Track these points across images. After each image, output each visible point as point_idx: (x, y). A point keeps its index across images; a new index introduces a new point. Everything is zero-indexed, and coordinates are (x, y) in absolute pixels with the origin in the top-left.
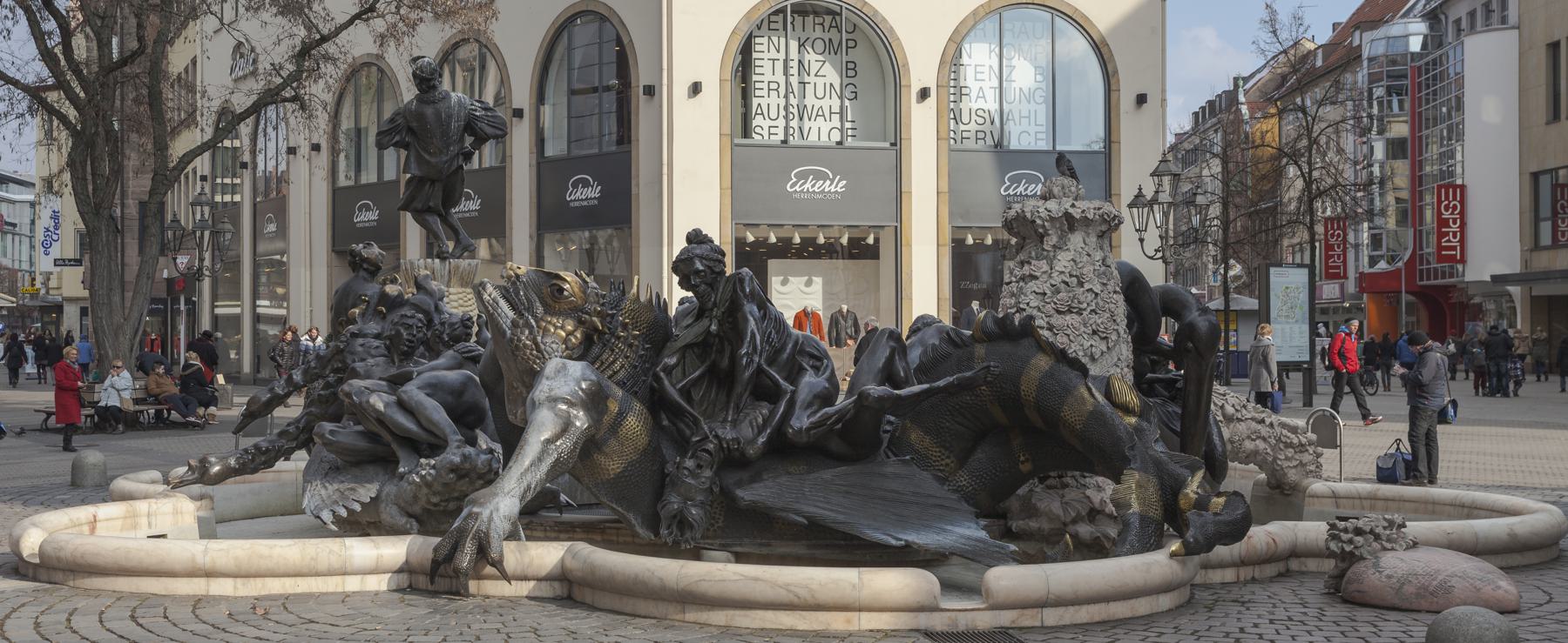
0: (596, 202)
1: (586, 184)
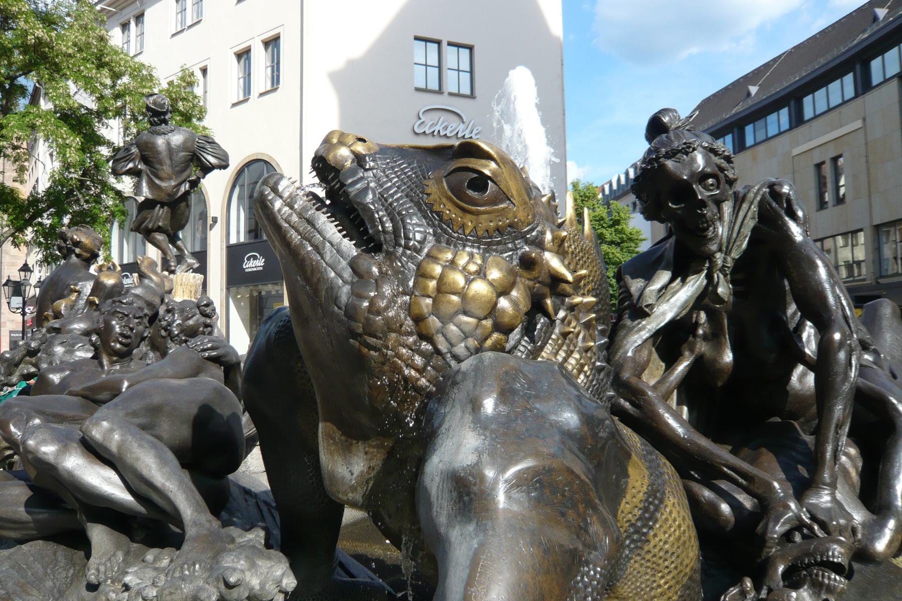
0: (261, 268)
1: (255, 258)
